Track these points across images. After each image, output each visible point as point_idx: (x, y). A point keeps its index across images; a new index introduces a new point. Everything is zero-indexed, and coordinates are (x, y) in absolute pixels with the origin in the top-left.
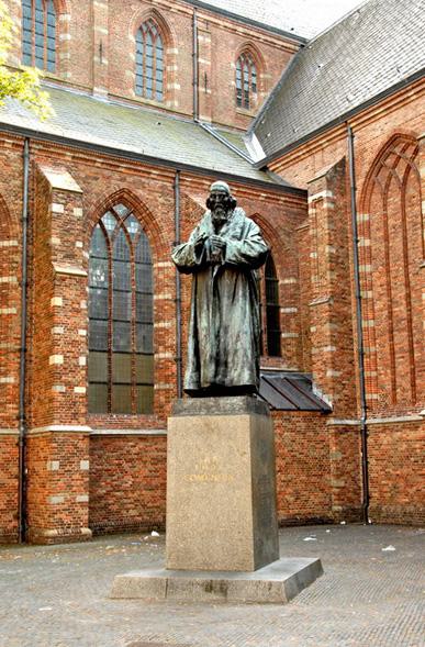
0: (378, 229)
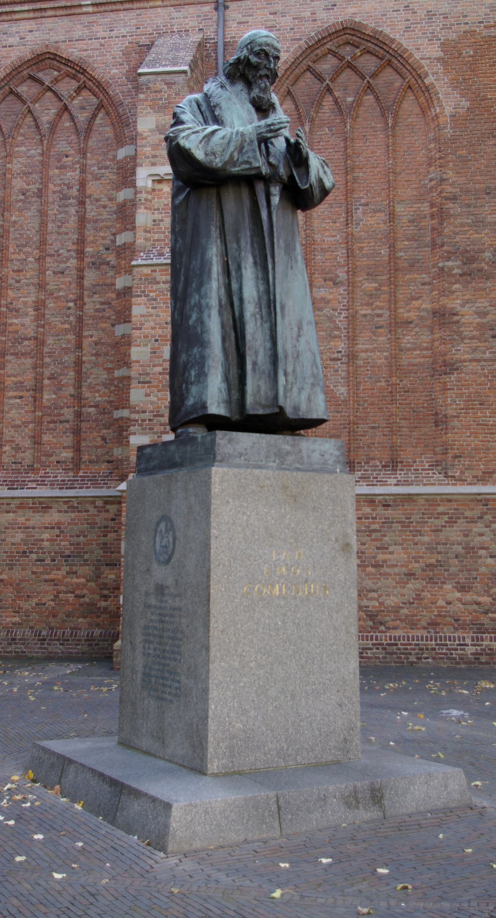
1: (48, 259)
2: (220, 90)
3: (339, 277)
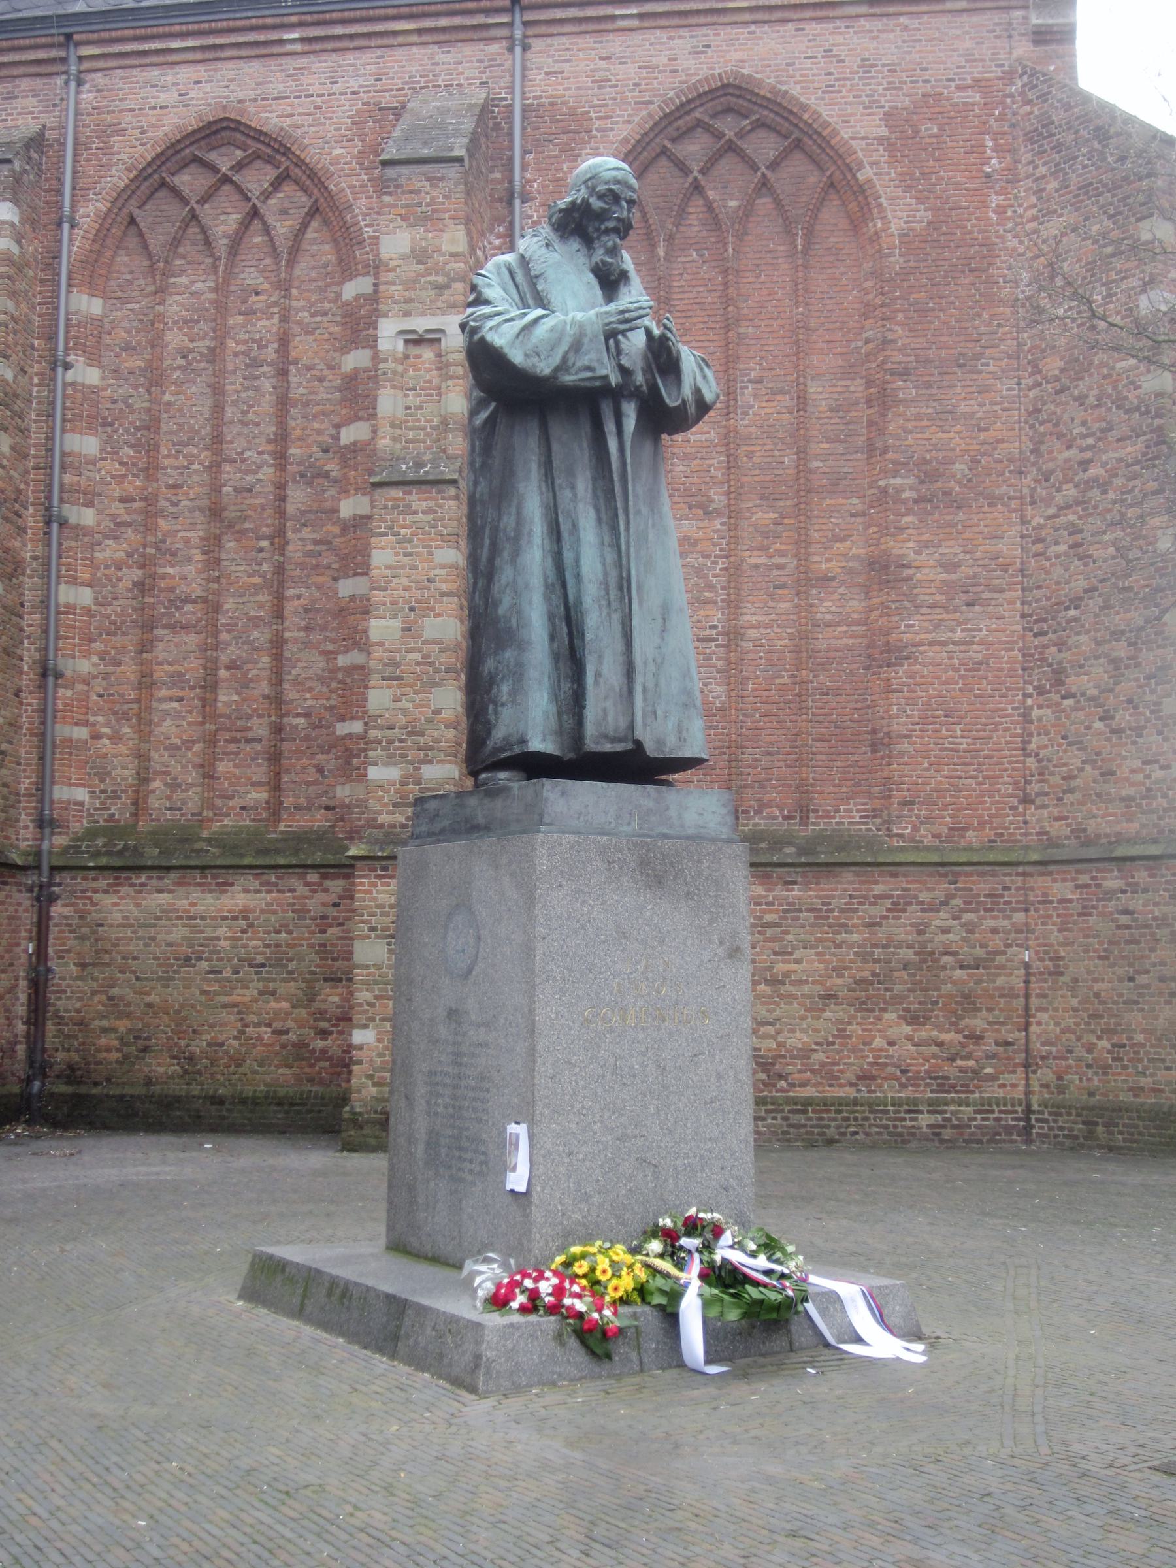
0: (127, 348)
1: (226, 467)
2: (544, 250)
3: (712, 501)
